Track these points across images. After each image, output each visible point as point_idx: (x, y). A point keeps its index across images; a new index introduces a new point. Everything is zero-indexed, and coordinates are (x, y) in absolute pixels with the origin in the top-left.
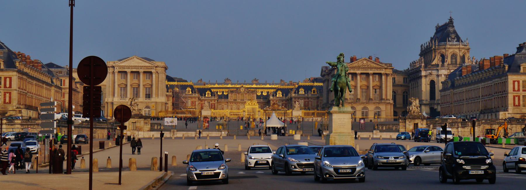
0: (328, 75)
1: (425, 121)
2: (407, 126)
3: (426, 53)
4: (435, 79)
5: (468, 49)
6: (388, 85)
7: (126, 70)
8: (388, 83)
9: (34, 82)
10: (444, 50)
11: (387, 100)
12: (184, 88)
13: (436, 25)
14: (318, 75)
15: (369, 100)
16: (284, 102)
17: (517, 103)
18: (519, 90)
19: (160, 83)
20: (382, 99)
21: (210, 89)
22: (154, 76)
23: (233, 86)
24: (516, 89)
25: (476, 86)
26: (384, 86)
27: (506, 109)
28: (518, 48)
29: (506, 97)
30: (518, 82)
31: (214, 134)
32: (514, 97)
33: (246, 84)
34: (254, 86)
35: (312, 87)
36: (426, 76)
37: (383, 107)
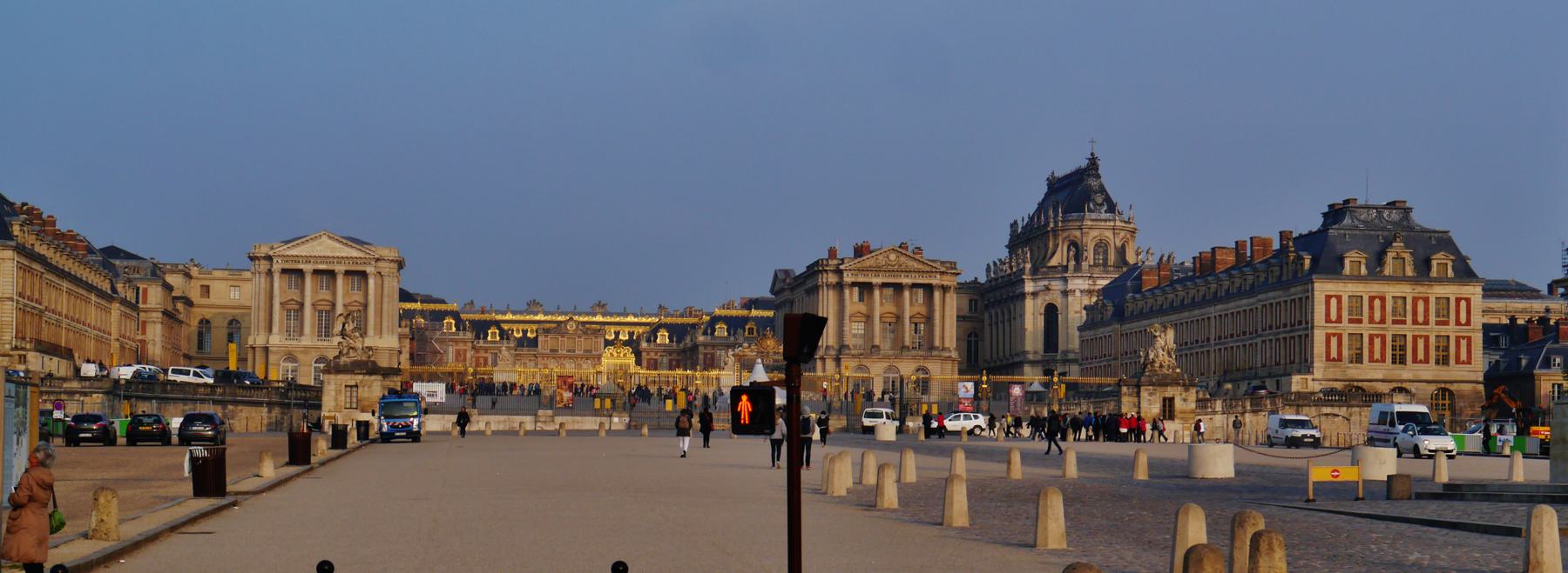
0: (792, 289)
1: (1193, 391)
2: (1144, 404)
3: (1029, 238)
4: (1059, 302)
5: (1133, 232)
6: (947, 314)
7: (301, 266)
8: (948, 309)
9: (65, 285)
10: (1078, 233)
11: (944, 349)
12: (438, 316)
13: (1047, 174)
14: (765, 292)
15: (901, 349)
16: (674, 356)
17: (1334, 354)
18: (1339, 320)
19: (386, 299)
20: (932, 348)
21: (497, 324)
22: (371, 282)
23: (548, 318)
24: (1334, 316)
25: (1197, 312)
26: (937, 315)
27: (1307, 368)
28: (1325, 215)
29: (1307, 338)
30: (1339, 298)
31: (590, 423)
32: (1328, 337)
33: (580, 314)
34: (599, 318)
35: (746, 320)
36: (1035, 294)
37: (934, 368)
